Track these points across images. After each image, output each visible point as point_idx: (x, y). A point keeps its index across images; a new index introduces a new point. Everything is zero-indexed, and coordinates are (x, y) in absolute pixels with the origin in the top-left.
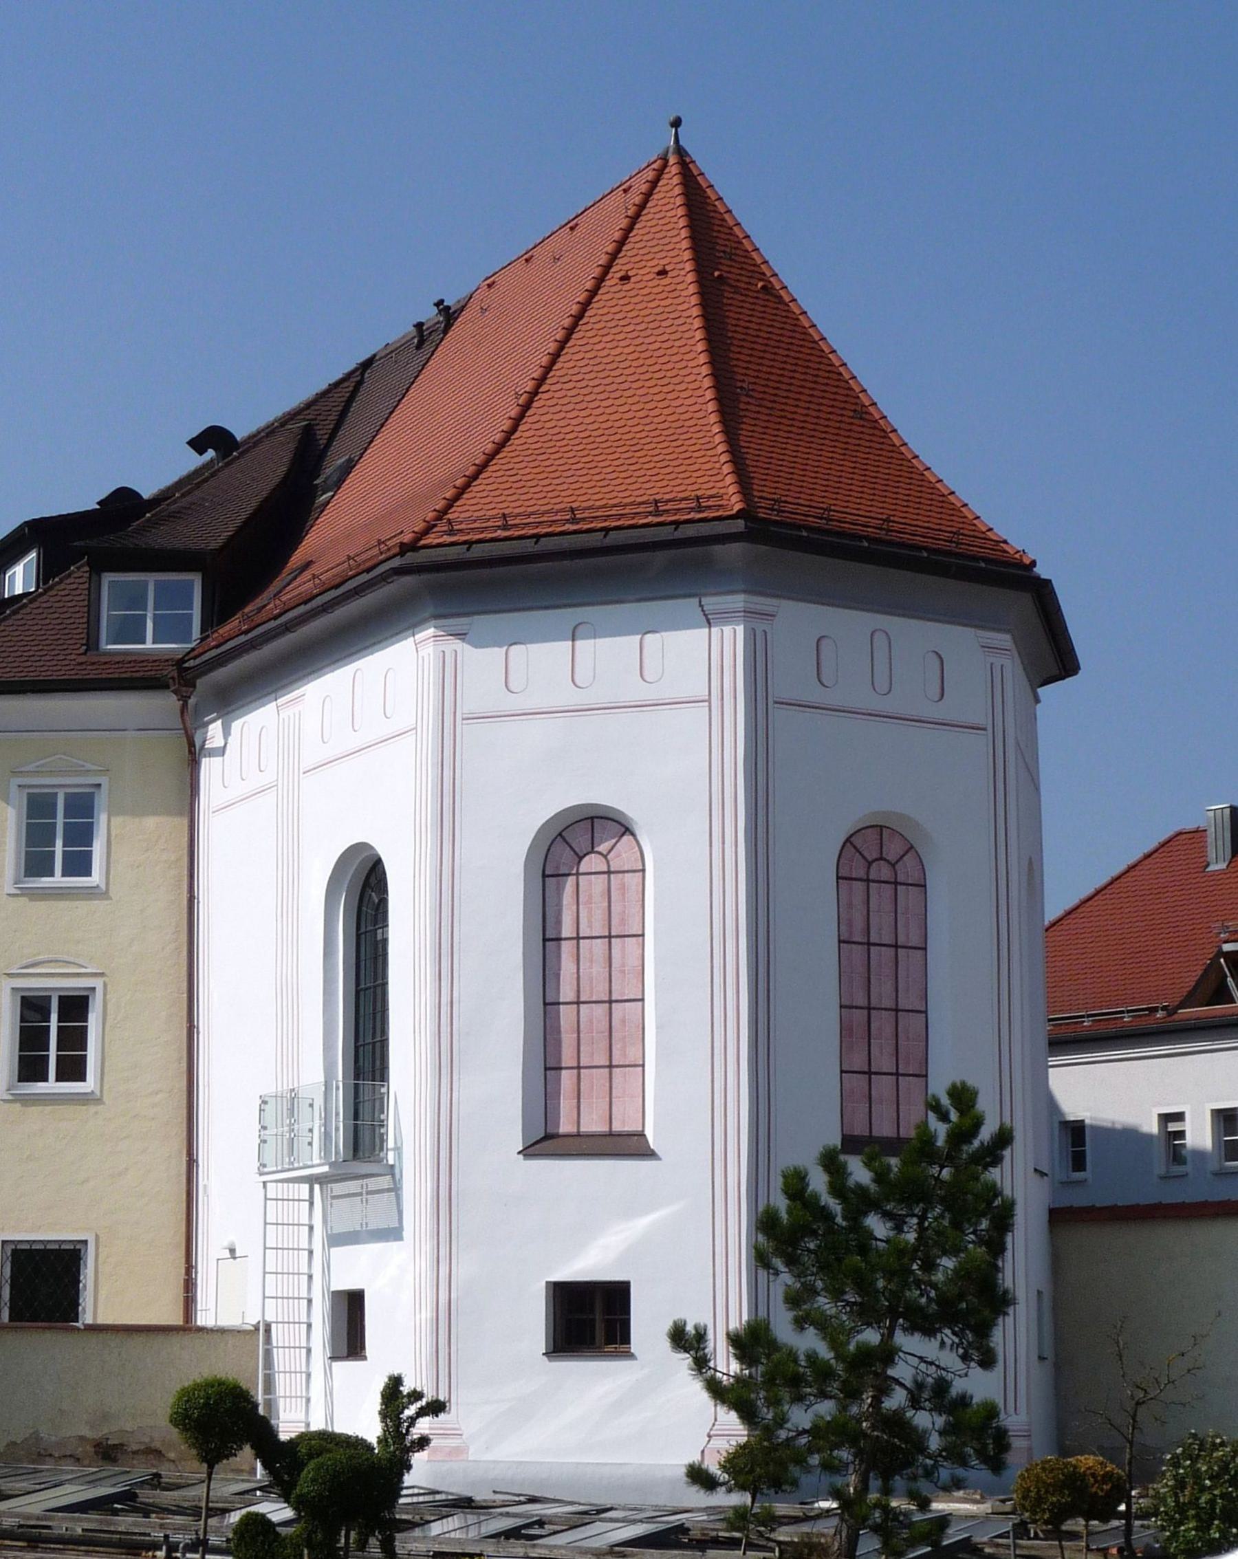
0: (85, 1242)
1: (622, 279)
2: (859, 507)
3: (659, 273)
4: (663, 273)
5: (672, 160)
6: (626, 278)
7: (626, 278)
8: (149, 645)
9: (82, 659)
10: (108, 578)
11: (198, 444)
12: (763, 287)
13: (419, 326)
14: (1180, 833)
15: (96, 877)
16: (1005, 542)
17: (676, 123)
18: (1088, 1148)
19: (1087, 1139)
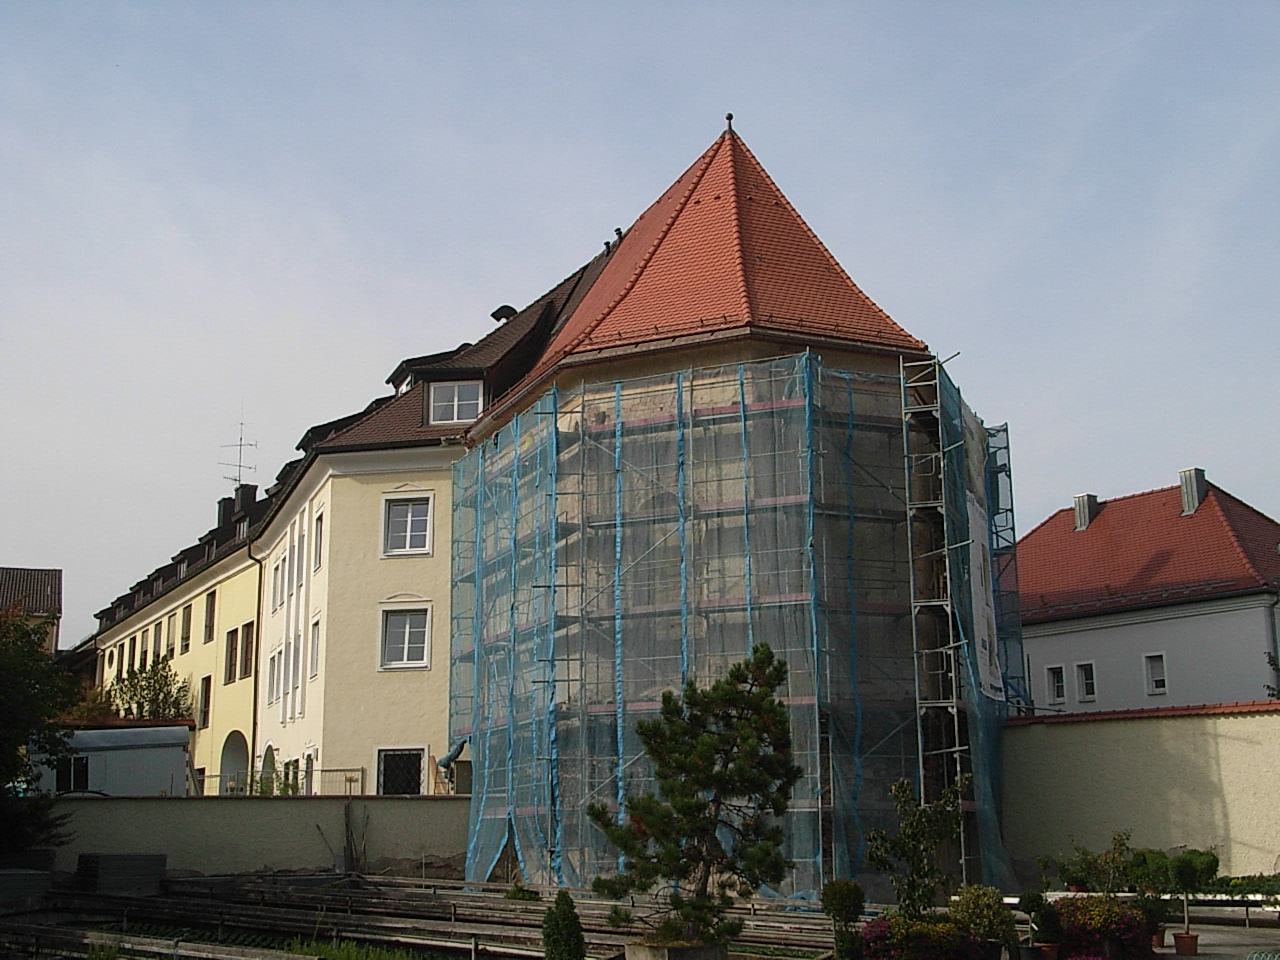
0: (423, 750)
1: (696, 203)
2: (822, 317)
3: (716, 198)
4: (718, 198)
5: (727, 137)
6: (698, 202)
7: (698, 202)
8: (455, 420)
9: (419, 430)
10: (433, 386)
11: (497, 316)
12: (776, 203)
13: (607, 244)
14: (1061, 511)
15: (427, 549)
16: (910, 336)
17: (730, 117)
18: (1095, 681)
19: (1064, 678)
